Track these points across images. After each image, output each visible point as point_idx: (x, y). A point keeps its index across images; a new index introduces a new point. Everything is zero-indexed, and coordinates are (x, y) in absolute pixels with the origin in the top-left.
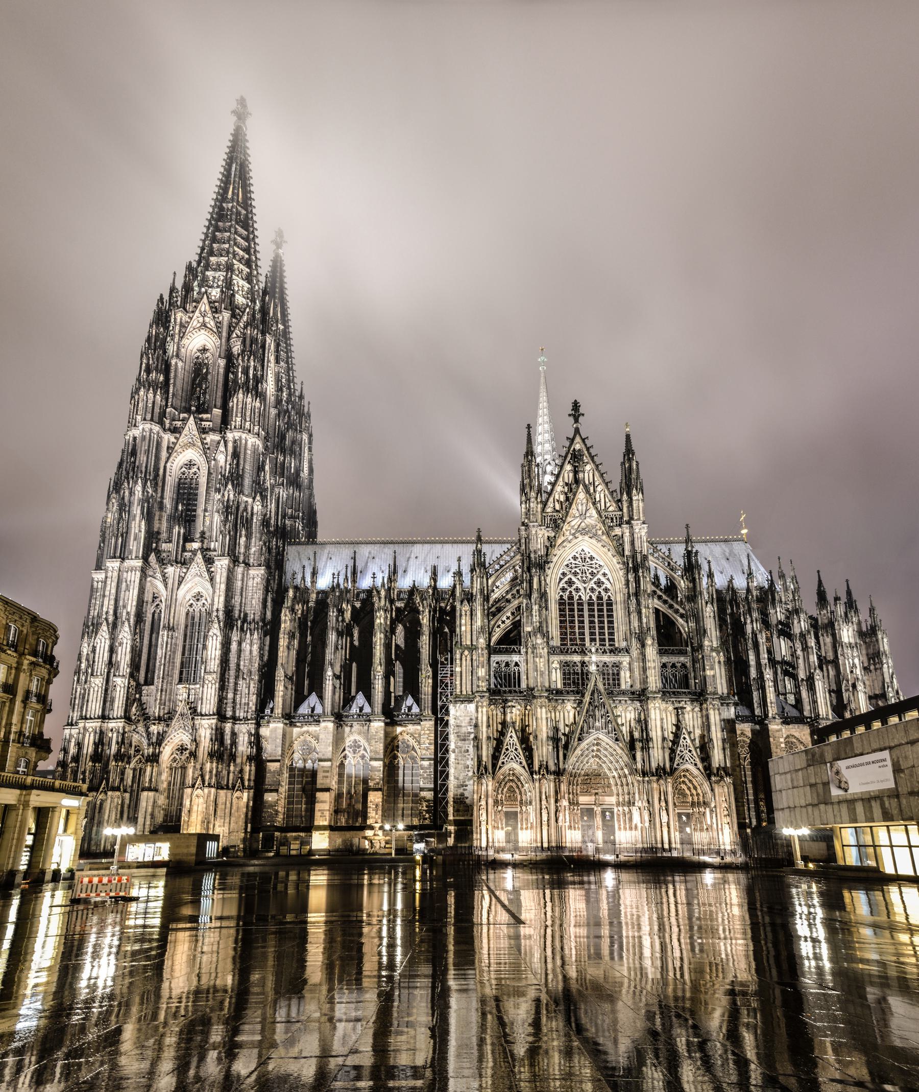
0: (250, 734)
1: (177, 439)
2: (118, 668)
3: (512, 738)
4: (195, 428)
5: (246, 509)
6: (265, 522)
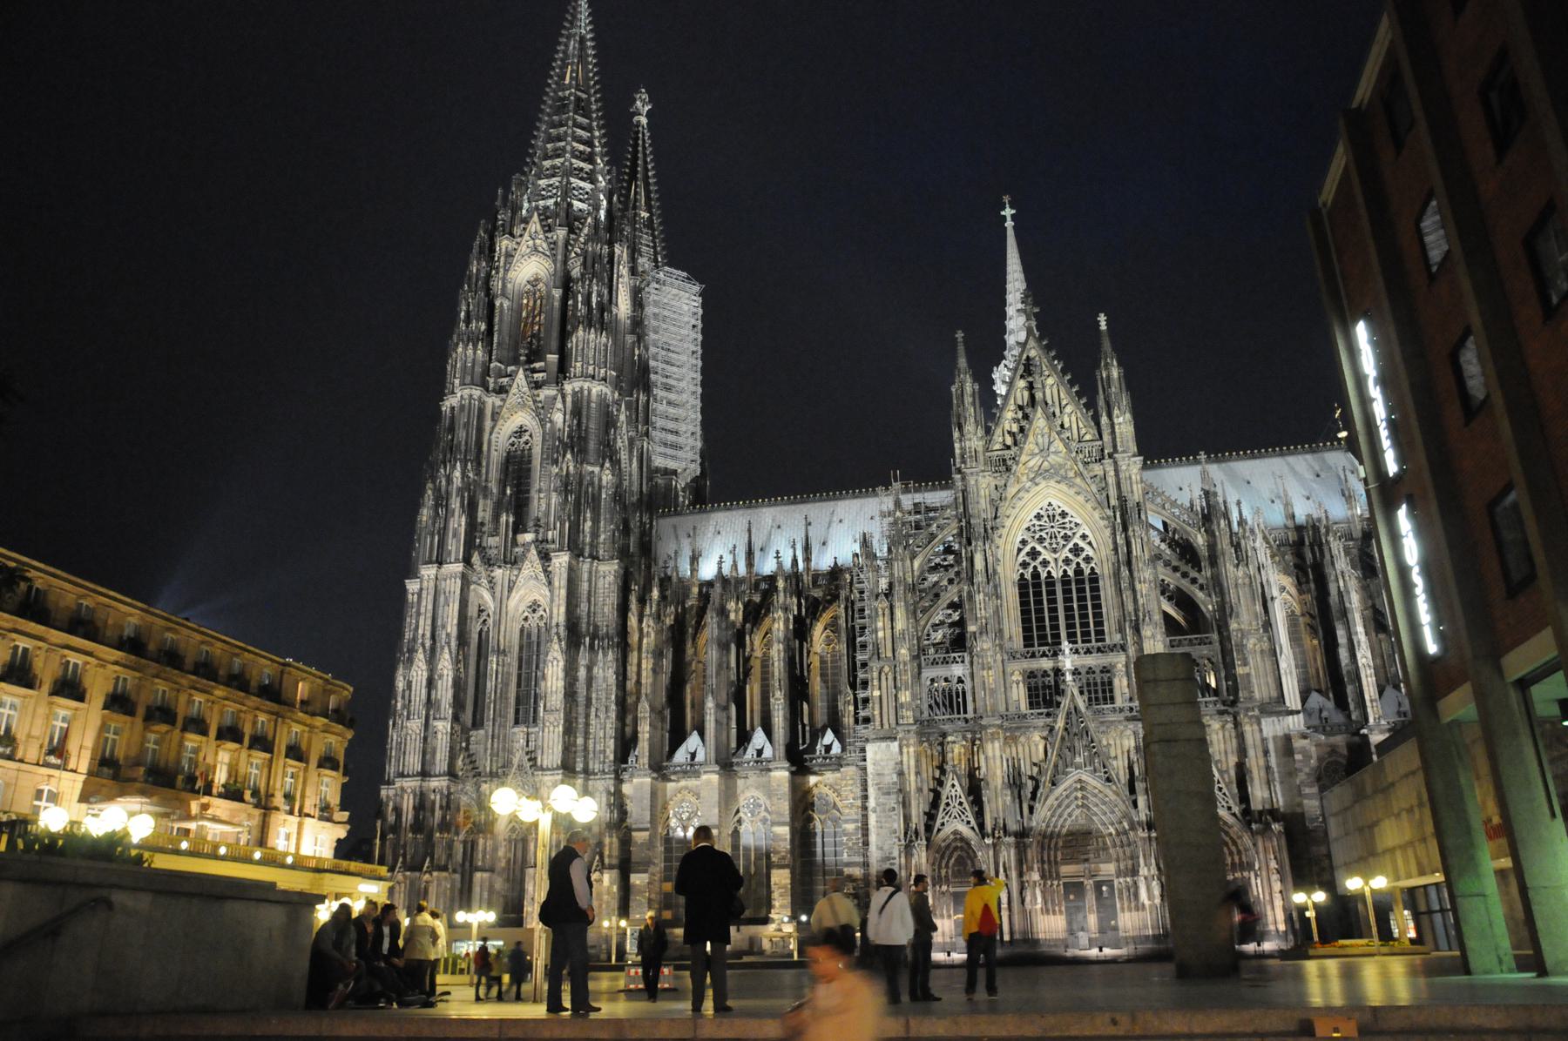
1: (503, 400)
2: (439, 709)
3: (954, 789)
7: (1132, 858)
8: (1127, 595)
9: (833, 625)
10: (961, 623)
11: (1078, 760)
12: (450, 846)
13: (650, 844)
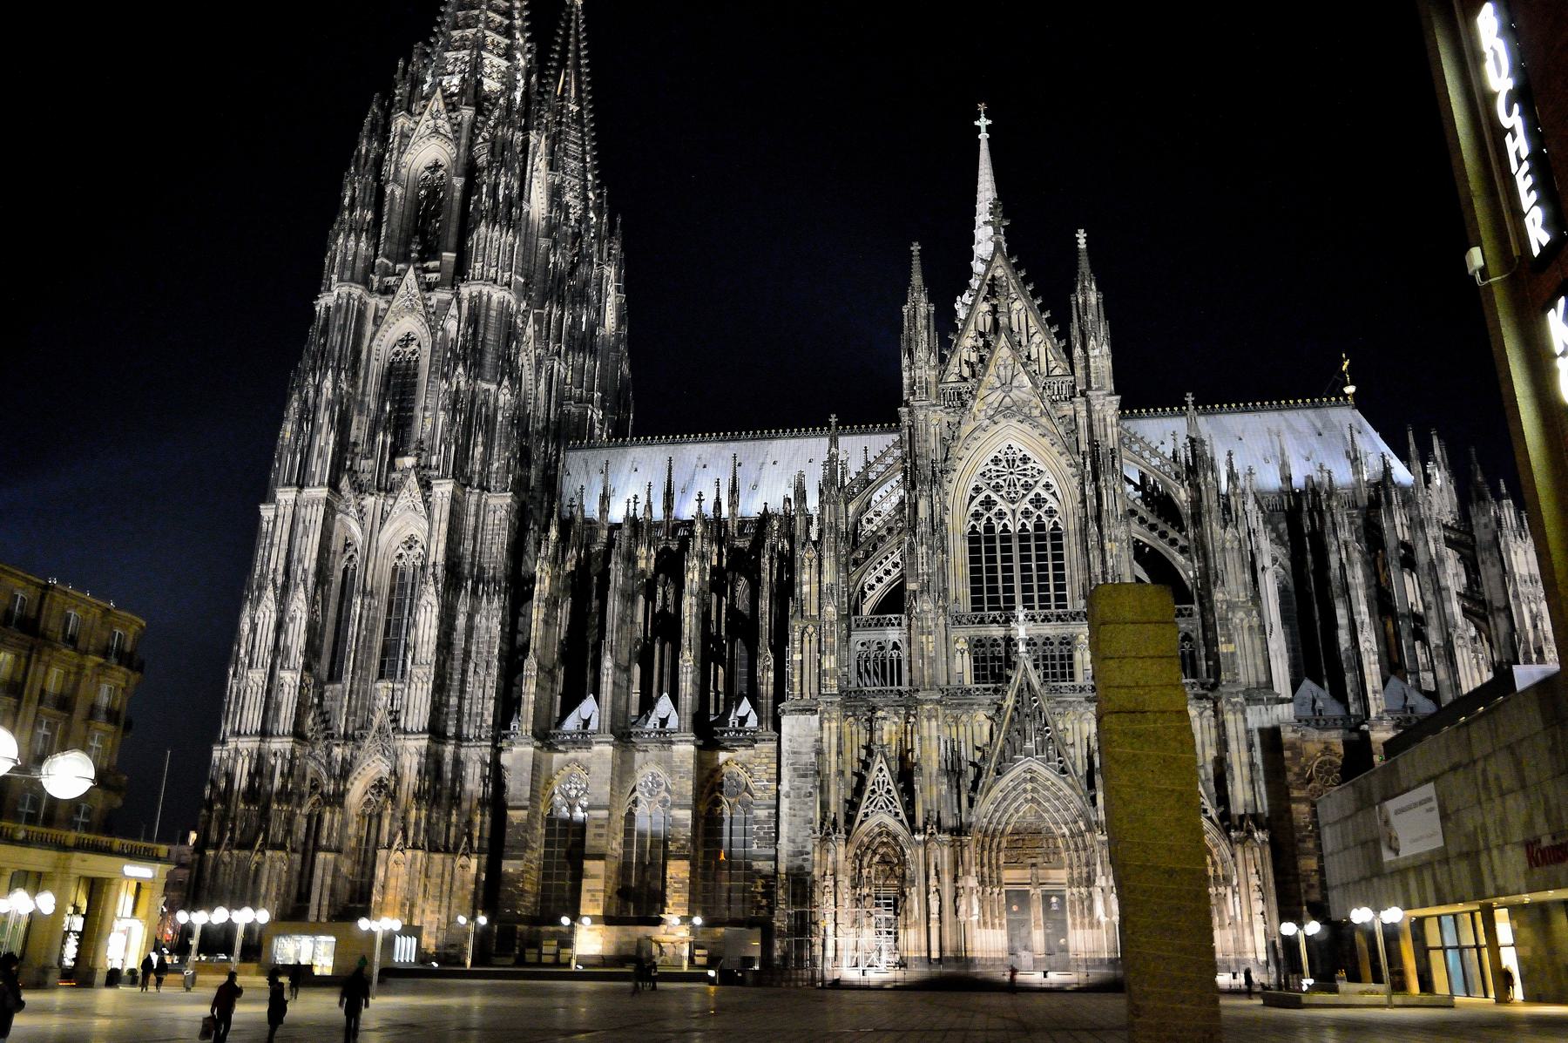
2: (287, 657)
3: (881, 774)
4: (415, 284)
5: (486, 403)
7: (1087, 864)
8: (1095, 555)
11: (1029, 745)
12: (290, 820)
13: (528, 825)
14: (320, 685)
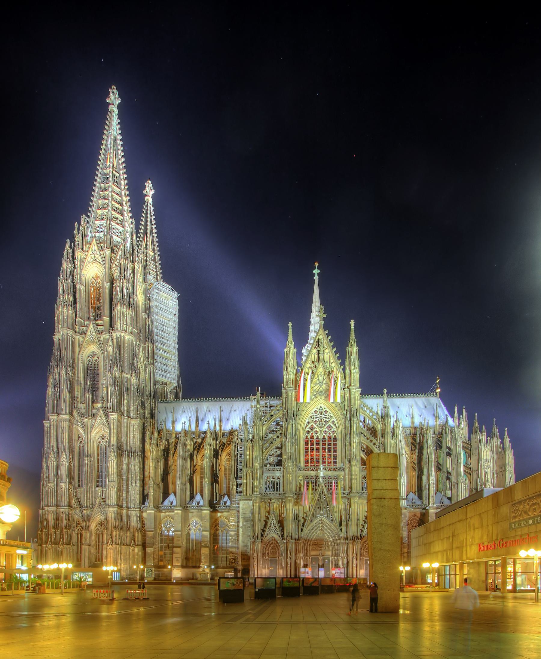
0: (137, 516)
1: (84, 338)
3: (273, 521)
4: (93, 331)
6: (139, 390)
7: (338, 550)
8: (348, 448)
9: (229, 454)
10: (280, 455)
11: (322, 512)
12: (71, 535)
13: (154, 537)
14: (75, 488)
